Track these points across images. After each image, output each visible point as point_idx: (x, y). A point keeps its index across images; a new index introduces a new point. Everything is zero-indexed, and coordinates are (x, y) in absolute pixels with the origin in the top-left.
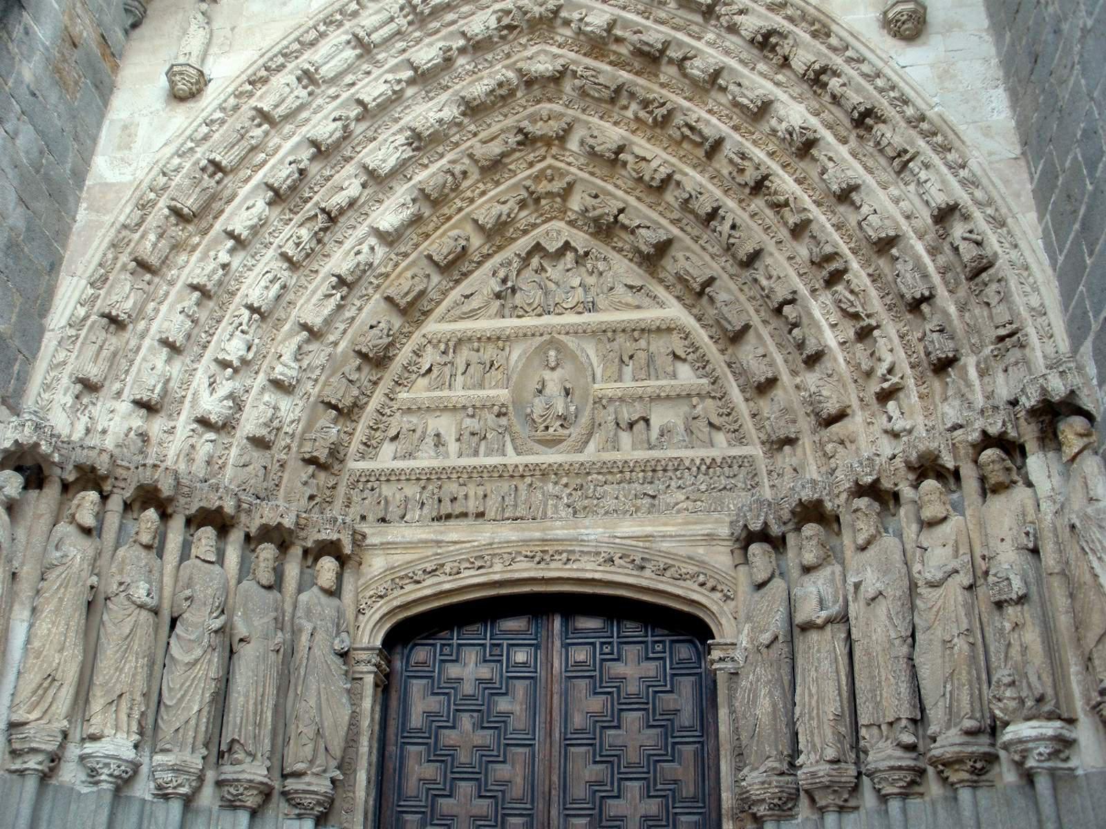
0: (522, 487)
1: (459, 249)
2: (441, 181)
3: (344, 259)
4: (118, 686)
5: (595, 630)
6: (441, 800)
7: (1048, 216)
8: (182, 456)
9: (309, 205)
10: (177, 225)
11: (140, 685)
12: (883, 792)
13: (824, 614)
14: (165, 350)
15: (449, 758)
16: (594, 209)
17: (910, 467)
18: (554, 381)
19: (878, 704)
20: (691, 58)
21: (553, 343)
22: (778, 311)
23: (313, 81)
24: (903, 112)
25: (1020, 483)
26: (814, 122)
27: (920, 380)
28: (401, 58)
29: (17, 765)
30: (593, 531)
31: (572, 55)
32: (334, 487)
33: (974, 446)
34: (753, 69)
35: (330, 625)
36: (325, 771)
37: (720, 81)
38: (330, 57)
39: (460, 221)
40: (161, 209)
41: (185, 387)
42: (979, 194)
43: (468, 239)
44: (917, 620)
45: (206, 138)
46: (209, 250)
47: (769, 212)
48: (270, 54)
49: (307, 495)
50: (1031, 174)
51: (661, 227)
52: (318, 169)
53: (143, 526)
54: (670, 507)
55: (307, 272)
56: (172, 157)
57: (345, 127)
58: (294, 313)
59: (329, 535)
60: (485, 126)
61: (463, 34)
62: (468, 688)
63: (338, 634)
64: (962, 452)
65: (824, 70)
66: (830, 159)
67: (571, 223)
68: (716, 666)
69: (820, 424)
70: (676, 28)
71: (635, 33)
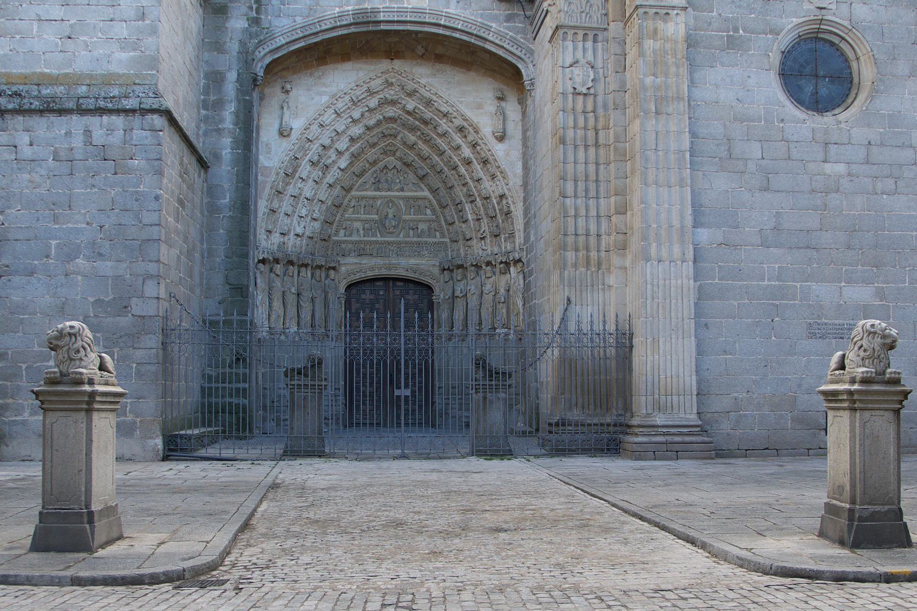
9: (321, 164)
13: (461, 295)
27: (491, 236)
30: (403, 261)
31: (401, 112)
43: (365, 166)
47: (457, 176)
59: (333, 265)
62: (367, 302)
70: (435, 115)
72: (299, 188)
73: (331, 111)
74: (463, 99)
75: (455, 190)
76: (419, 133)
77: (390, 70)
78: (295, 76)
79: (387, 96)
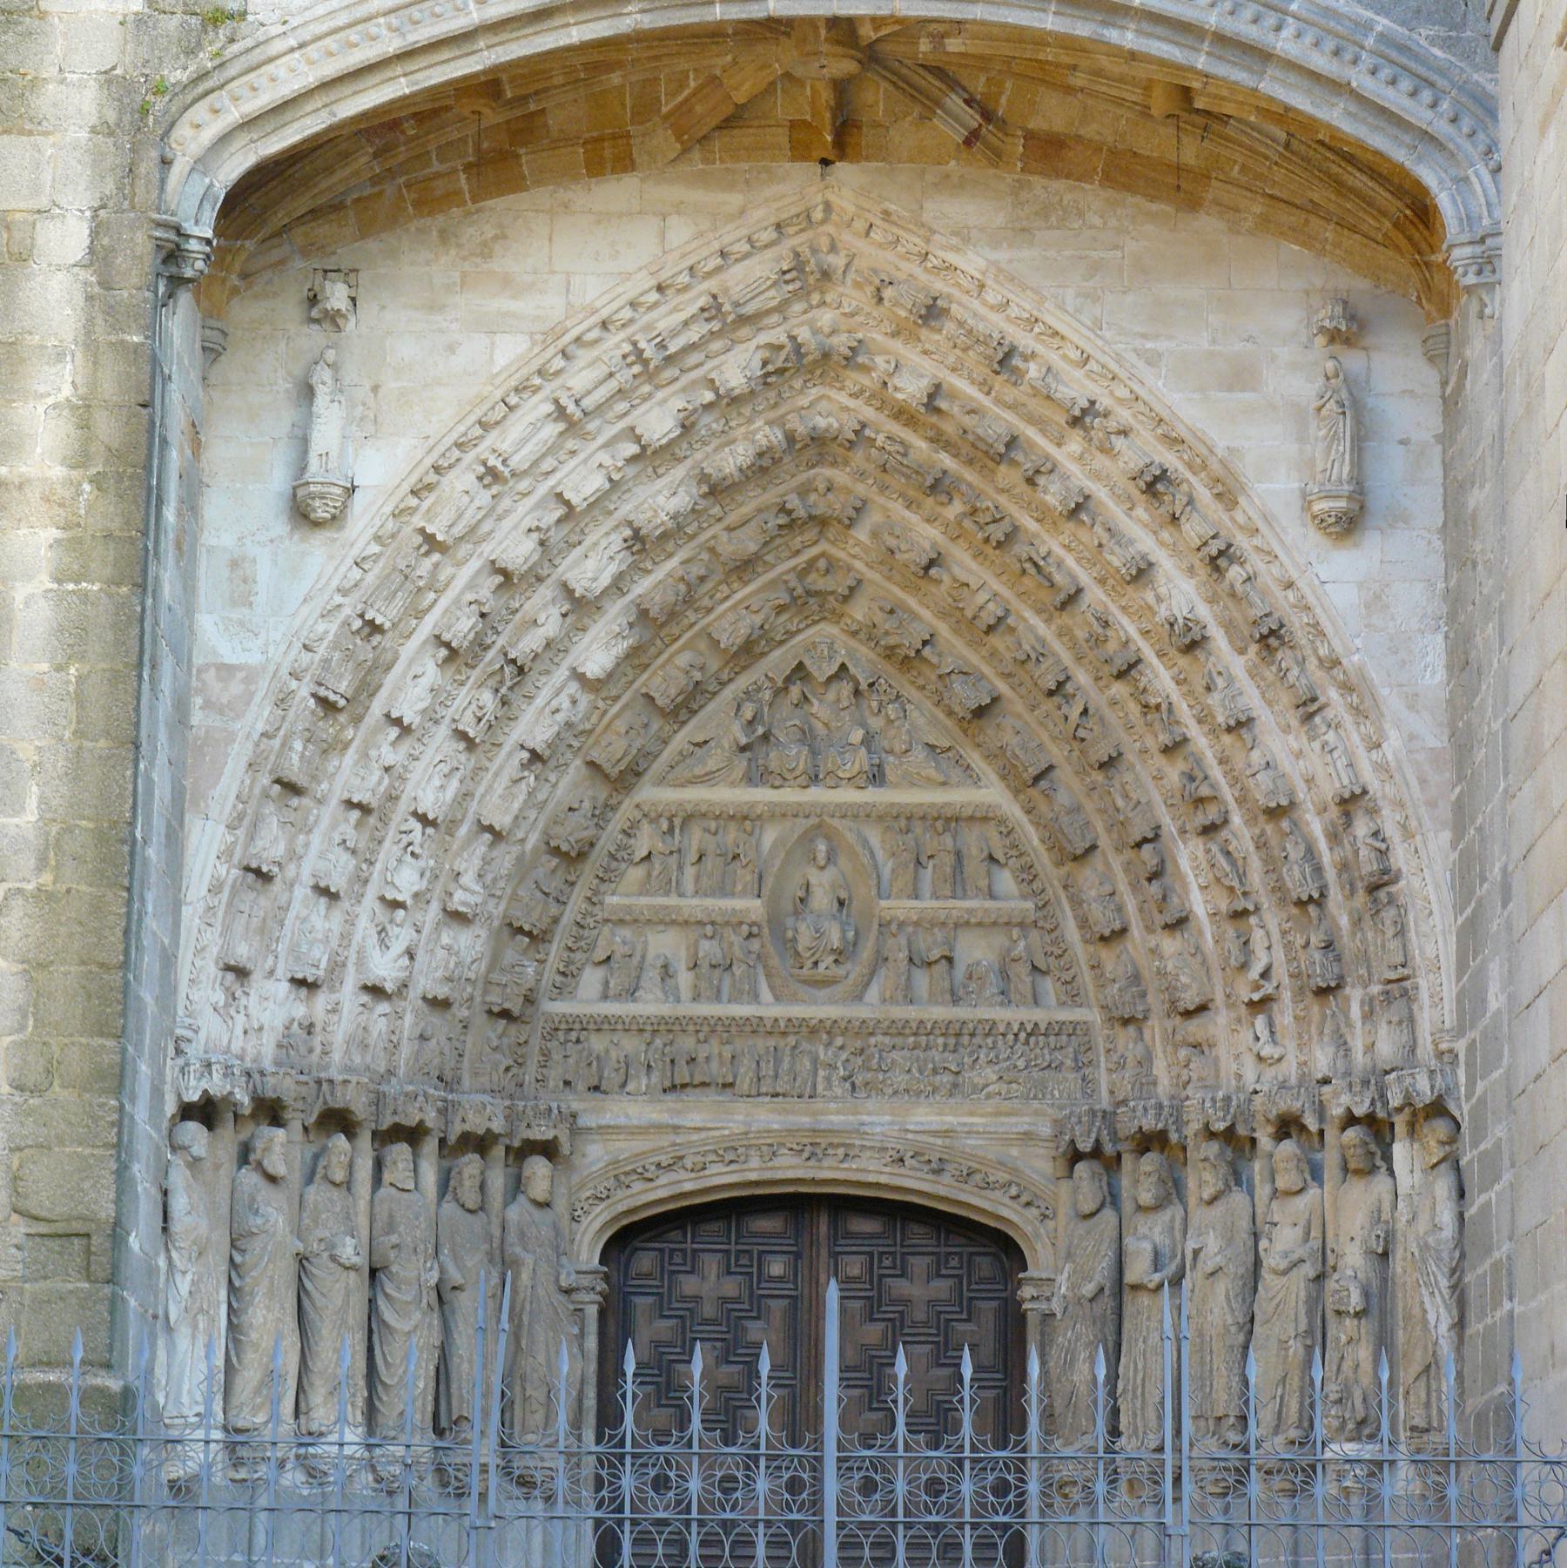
5: (872, 1236)
9: (491, 654)
13: (1157, 1277)
14: (323, 901)
18: (823, 883)
25: (1383, 1170)
26: (1204, 612)
27: (1299, 993)
29: (242, 1474)
39: (692, 638)
47: (1134, 709)
48: (441, 448)
49: (502, 1068)
51: (982, 677)
53: (334, 1160)
54: (977, 1089)
59: (541, 1132)
62: (709, 1310)
68: (1026, 1306)
72: (387, 769)
73: (537, 407)
74: (1161, 345)
75: (1128, 777)
76: (956, 508)
77: (818, 215)
78: (372, 245)
79: (804, 334)
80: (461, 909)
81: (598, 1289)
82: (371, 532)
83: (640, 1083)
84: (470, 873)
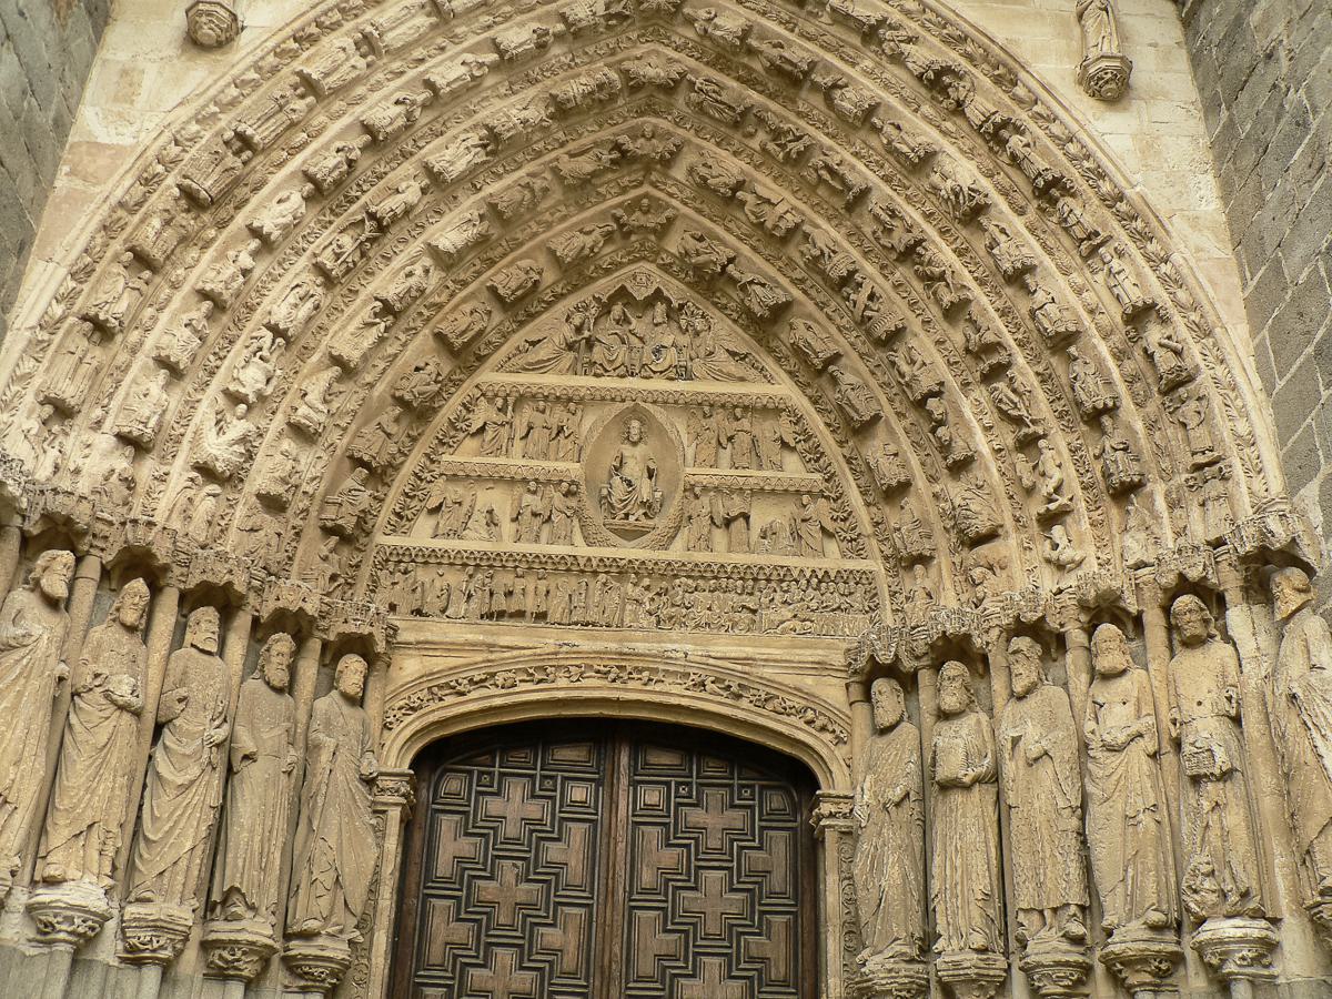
0: (596, 586)
1: (530, 284)
2: (518, 197)
3: (391, 281)
4: (89, 812)
6: (472, 971)
7: (1265, 332)
8: (174, 516)
9: (354, 207)
10: (188, 211)
11: (119, 812)
12: (1044, 991)
13: (971, 774)
14: (163, 373)
15: (485, 917)
16: (698, 254)
17: (1083, 606)
19: (1040, 885)
20: (841, 87)
21: (636, 413)
22: (920, 404)
23: (373, 50)
24: (1098, 187)
25: (1218, 638)
26: (985, 184)
27: (1094, 505)
28: (483, 36)
30: (681, 644)
31: (692, 63)
32: (357, 566)
33: (1165, 590)
34: (916, 111)
35: (354, 742)
36: (341, 932)
37: (875, 120)
38: (398, 22)
39: (533, 249)
40: (169, 187)
41: (183, 422)
42: (1182, 295)
43: (540, 273)
44: (1090, 788)
45: (233, 103)
46: (226, 249)
47: (918, 286)
50: (1244, 278)
51: (779, 285)
52: (370, 162)
53: (128, 601)
55: (345, 291)
56: (188, 122)
57: (409, 115)
58: (326, 341)
60: (575, 136)
61: (563, 18)
62: (511, 830)
63: (363, 753)
64: (1147, 594)
65: (1005, 124)
66: (1003, 231)
67: (665, 268)
69: (962, 543)
70: (826, 47)
71: (775, 46)
75: (913, 342)
80: (303, 421)
81: (403, 790)
82: (250, 59)
83: (459, 607)
84: (316, 392)
